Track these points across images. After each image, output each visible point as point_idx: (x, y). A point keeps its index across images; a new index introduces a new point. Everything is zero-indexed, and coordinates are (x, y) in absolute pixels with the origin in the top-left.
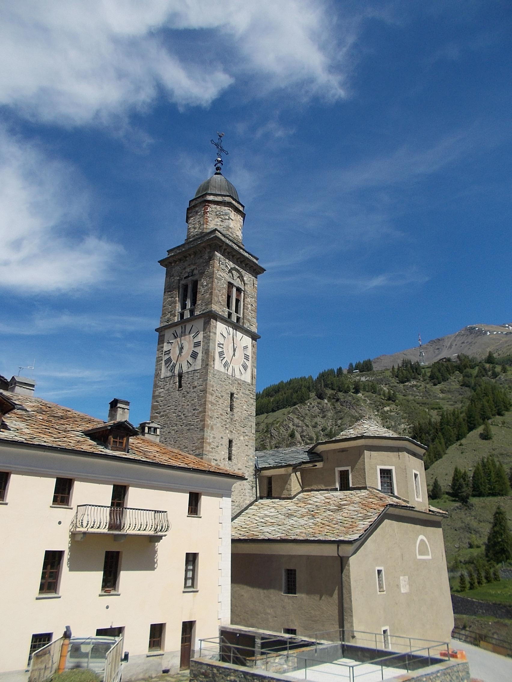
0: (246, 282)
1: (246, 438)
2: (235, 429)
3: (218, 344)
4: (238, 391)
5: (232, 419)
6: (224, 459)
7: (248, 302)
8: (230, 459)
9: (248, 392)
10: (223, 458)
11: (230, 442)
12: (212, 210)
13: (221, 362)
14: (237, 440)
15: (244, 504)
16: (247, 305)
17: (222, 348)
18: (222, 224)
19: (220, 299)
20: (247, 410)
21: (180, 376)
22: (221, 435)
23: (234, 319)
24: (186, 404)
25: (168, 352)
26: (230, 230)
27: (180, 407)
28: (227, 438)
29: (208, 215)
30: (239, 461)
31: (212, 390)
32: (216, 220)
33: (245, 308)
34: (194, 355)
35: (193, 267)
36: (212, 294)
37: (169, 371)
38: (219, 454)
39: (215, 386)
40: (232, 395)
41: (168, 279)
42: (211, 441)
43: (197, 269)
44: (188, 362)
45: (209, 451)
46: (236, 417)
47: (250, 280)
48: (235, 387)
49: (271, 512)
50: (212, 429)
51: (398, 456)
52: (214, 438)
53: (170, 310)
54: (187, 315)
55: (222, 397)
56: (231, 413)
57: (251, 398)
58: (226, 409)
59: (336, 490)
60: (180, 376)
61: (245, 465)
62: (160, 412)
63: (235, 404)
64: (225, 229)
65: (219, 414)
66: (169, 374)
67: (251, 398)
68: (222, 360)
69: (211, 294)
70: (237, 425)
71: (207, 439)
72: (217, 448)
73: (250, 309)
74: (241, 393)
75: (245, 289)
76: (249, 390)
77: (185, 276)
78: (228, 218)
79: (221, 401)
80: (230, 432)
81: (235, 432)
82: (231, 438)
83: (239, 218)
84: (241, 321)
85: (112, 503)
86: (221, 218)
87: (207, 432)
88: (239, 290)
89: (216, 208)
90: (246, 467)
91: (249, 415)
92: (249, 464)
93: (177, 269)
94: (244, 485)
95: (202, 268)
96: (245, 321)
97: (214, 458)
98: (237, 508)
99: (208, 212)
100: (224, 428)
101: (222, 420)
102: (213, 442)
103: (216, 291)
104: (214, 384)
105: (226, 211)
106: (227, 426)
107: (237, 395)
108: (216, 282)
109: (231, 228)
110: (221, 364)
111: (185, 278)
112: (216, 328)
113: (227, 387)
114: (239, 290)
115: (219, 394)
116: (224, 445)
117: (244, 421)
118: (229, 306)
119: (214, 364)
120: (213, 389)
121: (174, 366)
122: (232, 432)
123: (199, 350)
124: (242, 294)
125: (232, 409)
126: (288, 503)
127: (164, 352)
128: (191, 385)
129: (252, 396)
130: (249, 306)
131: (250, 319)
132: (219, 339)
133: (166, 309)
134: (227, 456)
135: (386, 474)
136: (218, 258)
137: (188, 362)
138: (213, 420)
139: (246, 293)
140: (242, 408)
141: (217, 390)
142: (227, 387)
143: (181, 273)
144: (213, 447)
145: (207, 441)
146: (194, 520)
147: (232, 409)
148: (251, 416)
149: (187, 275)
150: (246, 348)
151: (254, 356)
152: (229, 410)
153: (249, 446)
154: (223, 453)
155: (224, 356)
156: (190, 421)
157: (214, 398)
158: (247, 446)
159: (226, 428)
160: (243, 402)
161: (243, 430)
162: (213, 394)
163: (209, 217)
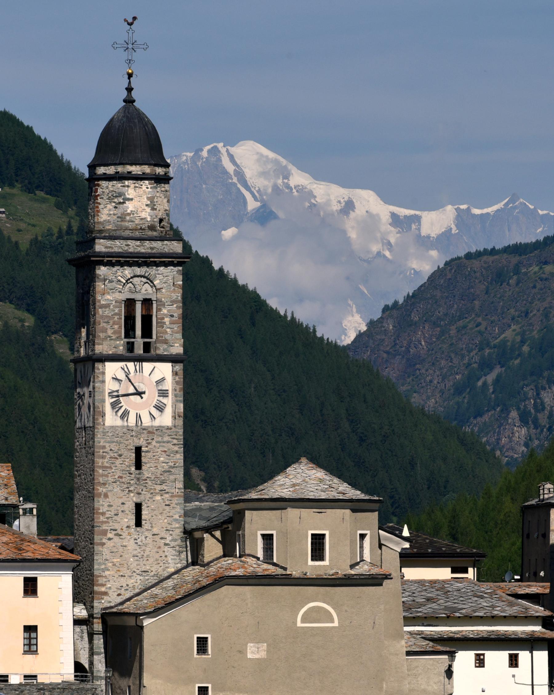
1: (167, 496)
4: (150, 441)
5: (138, 479)
9: (166, 439)
11: (138, 507)
12: (103, 192)
13: (116, 415)
14: (149, 502)
15: (165, 572)
20: (167, 461)
22: (121, 501)
26: (128, 218)
28: (131, 502)
30: (154, 525)
31: (103, 452)
38: (119, 522)
39: (107, 446)
40: (138, 451)
42: (104, 510)
47: (168, 280)
48: (142, 439)
50: (106, 496)
51: (280, 519)
52: (110, 506)
55: (120, 455)
56: (138, 472)
57: (174, 445)
58: (128, 469)
61: (165, 529)
65: (116, 477)
67: (174, 445)
68: (117, 412)
70: (150, 483)
71: (99, 509)
72: (116, 517)
73: (167, 323)
74: (154, 443)
78: (122, 201)
79: (118, 462)
80: (137, 495)
82: (138, 501)
86: (115, 202)
87: (99, 502)
88: (147, 302)
91: (171, 467)
92: (173, 526)
94: (164, 551)
97: (111, 528)
98: (152, 578)
99: (98, 195)
100: (127, 492)
101: (123, 482)
106: (130, 489)
107: (147, 447)
109: (129, 214)
112: (103, 373)
115: (115, 454)
119: (104, 421)
120: (105, 450)
122: (139, 494)
124: (155, 306)
129: (175, 441)
134: (134, 522)
135: (268, 539)
138: (107, 486)
141: (111, 450)
142: (126, 442)
144: (110, 516)
145: (99, 511)
146: (31, 600)
148: (174, 467)
151: (178, 387)
152: (133, 469)
155: (120, 405)
157: (106, 460)
158: (169, 505)
159: (129, 491)
161: (158, 488)
162: (105, 456)
163: (99, 204)
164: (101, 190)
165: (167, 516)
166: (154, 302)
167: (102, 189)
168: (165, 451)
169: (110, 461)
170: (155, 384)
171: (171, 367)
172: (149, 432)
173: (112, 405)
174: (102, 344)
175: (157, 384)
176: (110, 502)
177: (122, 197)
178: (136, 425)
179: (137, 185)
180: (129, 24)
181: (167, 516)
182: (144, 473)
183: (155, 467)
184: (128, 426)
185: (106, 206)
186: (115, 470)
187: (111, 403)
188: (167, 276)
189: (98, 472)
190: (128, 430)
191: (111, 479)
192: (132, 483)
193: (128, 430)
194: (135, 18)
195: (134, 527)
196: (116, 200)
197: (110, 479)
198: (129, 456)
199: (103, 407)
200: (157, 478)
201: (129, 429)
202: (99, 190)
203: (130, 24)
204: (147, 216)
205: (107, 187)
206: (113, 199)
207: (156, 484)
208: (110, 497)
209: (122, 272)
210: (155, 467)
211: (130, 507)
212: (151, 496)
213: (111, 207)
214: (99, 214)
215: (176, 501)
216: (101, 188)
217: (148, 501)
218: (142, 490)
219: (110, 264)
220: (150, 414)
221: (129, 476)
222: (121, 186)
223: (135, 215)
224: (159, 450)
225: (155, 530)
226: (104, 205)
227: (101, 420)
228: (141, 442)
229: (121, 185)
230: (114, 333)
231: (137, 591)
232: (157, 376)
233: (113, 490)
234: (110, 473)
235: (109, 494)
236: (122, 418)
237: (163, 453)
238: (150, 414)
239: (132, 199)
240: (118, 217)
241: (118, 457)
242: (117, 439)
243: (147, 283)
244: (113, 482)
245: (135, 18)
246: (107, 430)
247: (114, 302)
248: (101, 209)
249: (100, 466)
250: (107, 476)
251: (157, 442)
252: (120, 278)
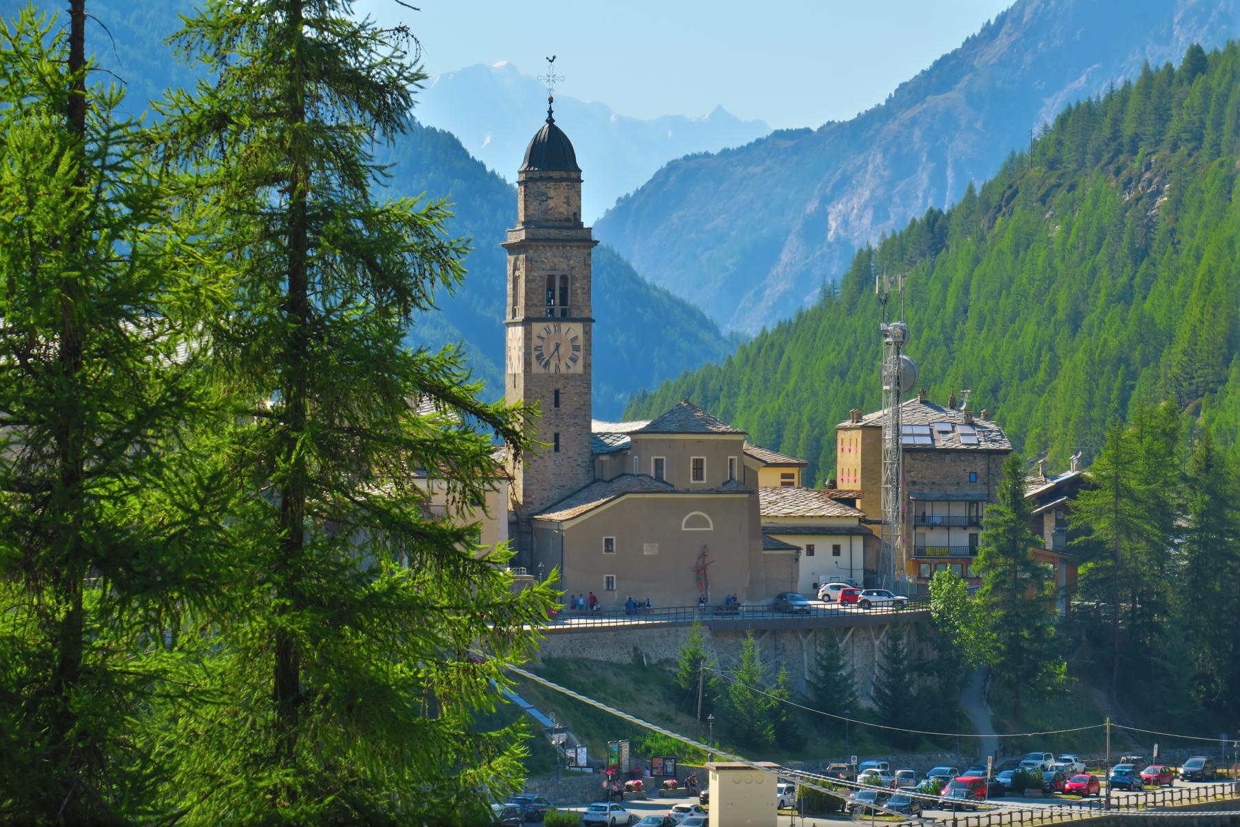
9: (579, 383)
32: (535, 203)
40: (557, 392)
74: (569, 387)
125: (557, 404)
147: (557, 404)
161: (572, 421)
194: (554, 57)
201: (550, 376)
203: (551, 61)
225: (570, 454)
228: (559, 386)
231: (555, 501)
232: (571, 335)
245: (554, 57)
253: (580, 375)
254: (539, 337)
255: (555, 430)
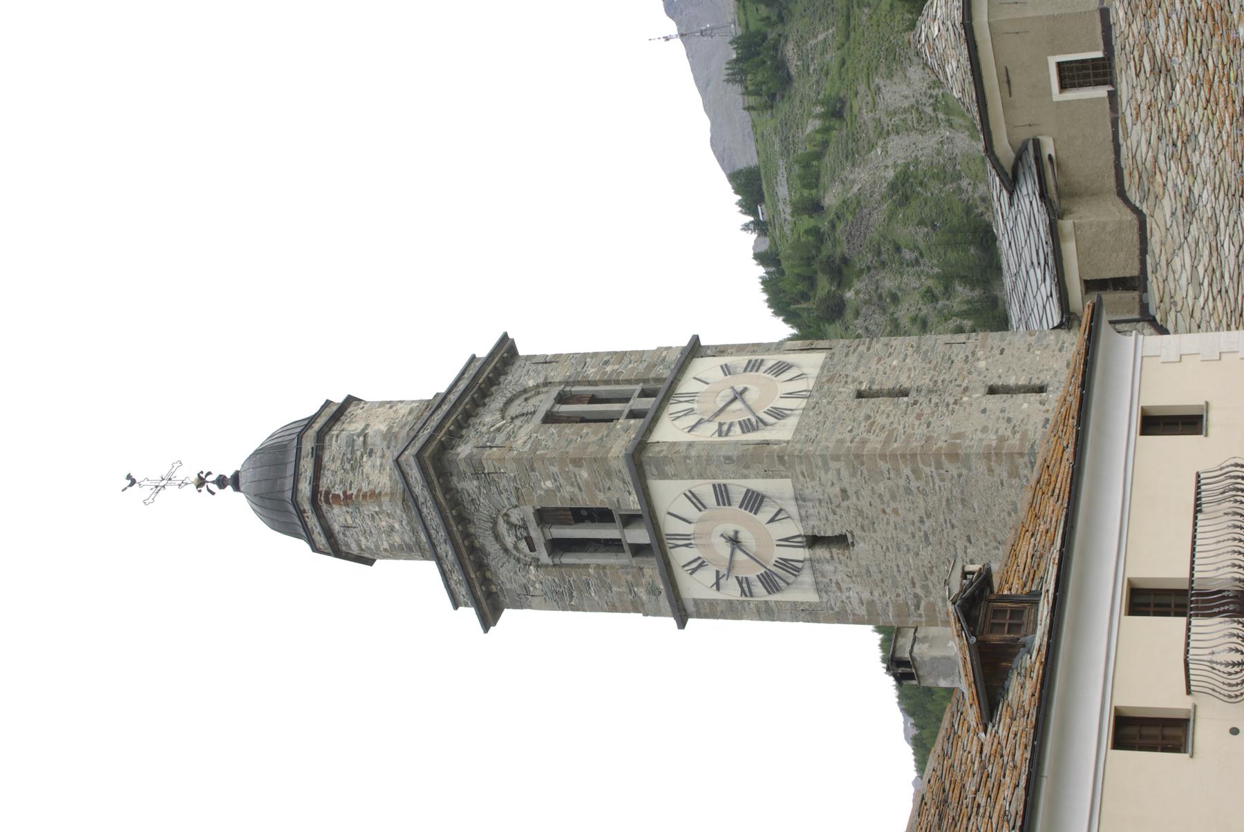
0: (541, 380)
1: (980, 354)
2: (958, 382)
3: (720, 435)
4: (850, 380)
5: (930, 391)
6: (1042, 403)
7: (595, 373)
8: (1041, 389)
10: (1041, 407)
12: (341, 482)
16: (605, 373)
17: (731, 425)
18: (379, 454)
19: (592, 438)
20: (902, 356)
21: (813, 541)
23: (648, 403)
24: (893, 518)
25: (745, 585)
27: (901, 535)
29: (354, 491)
30: (1046, 367)
31: (852, 442)
32: (367, 468)
33: (614, 377)
34: (754, 501)
35: (502, 527)
36: (581, 459)
37: (800, 579)
39: (839, 437)
41: (536, 600)
42: (994, 437)
43: (506, 515)
44: (772, 520)
45: (1022, 440)
46: (926, 381)
48: (841, 389)
49: (1183, 266)
50: (960, 435)
53: (624, 589)
54: (638, 535)
56: (913, 394)
57: (868, 349)
58: (903, 406)
59: (1113, 96)
60: (813, 541)
62: (916, 596)
63: (889, 385)
64: (393, 444)
65: (917, 423)
66: (807, 577)
67: (868, 349)
69: (577, 462)
70: (947, 377)
71: (990, 446)
73: (616, 367)
74: (856, 374)
75: (560, 383)
76: (847, 355)
77: (527, 550)
78: (361, 439)
79: (881, 420)
81: (966, 381)
82: (983, 390)
83: (360, 411)
84: (652, 385)
85: (1177, 614)
86: (362, 456)
88: (562, 399)
89: (335, 473)
90: (1060, 350)
93: (505, 573)
95: (504, 496)
96: (652, 375)
97: (1040, 427)
99: (345, 493)
100: (957, 407)
102: (997, 432)
103: (570, 449)
104: (834, 439)
105: (344, 443)
106: (951, 401)
107: (861, 383)
108: (545, 451)
109: (390, 428)
110: (777, 427)
111: (532, 549)
112: (674, 444)
113: (842, 408)
114: (562, 399)
115: (863, 424)
116: (1005, 405)
117: (934, 363)
118: (609, 419)
119: (778, 442)
121: (784, 563)
122: (966, 389)
123: (738, 487)
126: (1154, 226)
127: (744, 598)
128: (839, 506)
130: (609, 369)
131: (645, 364)
132: (707, 433)
133: (621, 601)
136: (475, 450)
137: (772, 520)
139: (571, 380)
140: (898, 369)
141: (850, 431)
142: (842, 408)
143: (518, 560)
144: (1009, 430)
146: (1214, 420)
149: (523, 545)
150: (726, 370)
152: (906, 399)
153: (1003, 345)
154: (1025, 405)
156: (940, 500)
159: (955, 403)
160: (881, 368)
161: (958, 364)
163: (359, 490)
164: (337, 486)
165: (1029, 350)
166: (568, 389)
167: (335, 484)
168: (880, 360)
169: (877, 431)
170: (729, 377)
171: (704, 358)
172: (830, 380)
173: (749, 431)
174: (611, 447)
175: (730, 374)
176: (976, 430)
177: (355, 437)
178: (808, 398)
179: (348, 420)
180: (131, 485)
181: (1029, 350)
182: (919, 384)
183: (910, 369)
184: (804, 409)
185: (365, 476)
186: (899, 424)
187: (743, 432)
188: (528, 372)
189: (898, 448)
190: (814, 408)
191: (920, 431)
192: (937, 401)
193: (814, 408)
194: (129, 477)
195: (1044, 394)
196: (359, 453)
197: (921, 430)
198: (873, 406)
199: (747, 443)
200: (935, 367)
202: (337, 493)
203: (133, 482)
204: (409, 407)
205: (335, 473)
206: (356, 459)
207: (950, 368)
208: (963, 430)
209: (484, 425)
210: (910, 369)
211: (994, 402)
212: (975, 375)
213: (370, 463)
214: (377, 492)
215: (995, 341)
216: (333, 487)
217: (985, 377)
218: (959, 386)
219: (455, 436)
220: (791, 380)
221: (921, 404)
222: (336, 441)
223: (397, 421)
224: (874, 367)
226: (363, 480)
227: (775, 447)
229: (334, 442)
230: (595, 433)
233: (947, 426)
234: (905, 432)
235: (954, 431)
236: (783, 416)
237: (882, 361)
238: (791, 380)
239: (367, 426)
240: (389, 448)
241: (871, 420)
242: (828, 423)
243: (526, 400)
244: (928, 427)
246: (803, 437)
247: (535, 435)
248: (370, 487)
249: (884, 445)
250: (909, 437)
251: (856, 369)
252: (492, 429)
253: (832, 357)
254: (692, 429)
255: (978, 394)
